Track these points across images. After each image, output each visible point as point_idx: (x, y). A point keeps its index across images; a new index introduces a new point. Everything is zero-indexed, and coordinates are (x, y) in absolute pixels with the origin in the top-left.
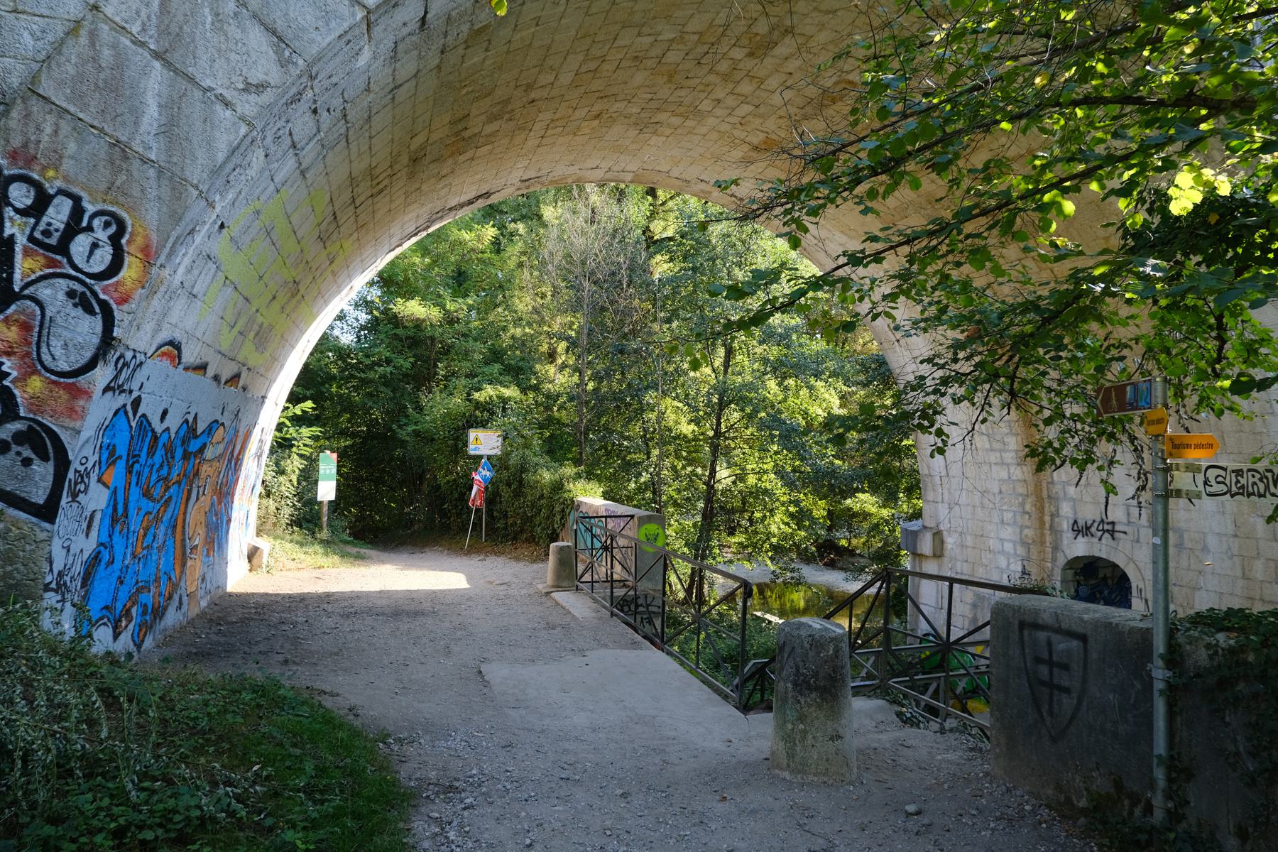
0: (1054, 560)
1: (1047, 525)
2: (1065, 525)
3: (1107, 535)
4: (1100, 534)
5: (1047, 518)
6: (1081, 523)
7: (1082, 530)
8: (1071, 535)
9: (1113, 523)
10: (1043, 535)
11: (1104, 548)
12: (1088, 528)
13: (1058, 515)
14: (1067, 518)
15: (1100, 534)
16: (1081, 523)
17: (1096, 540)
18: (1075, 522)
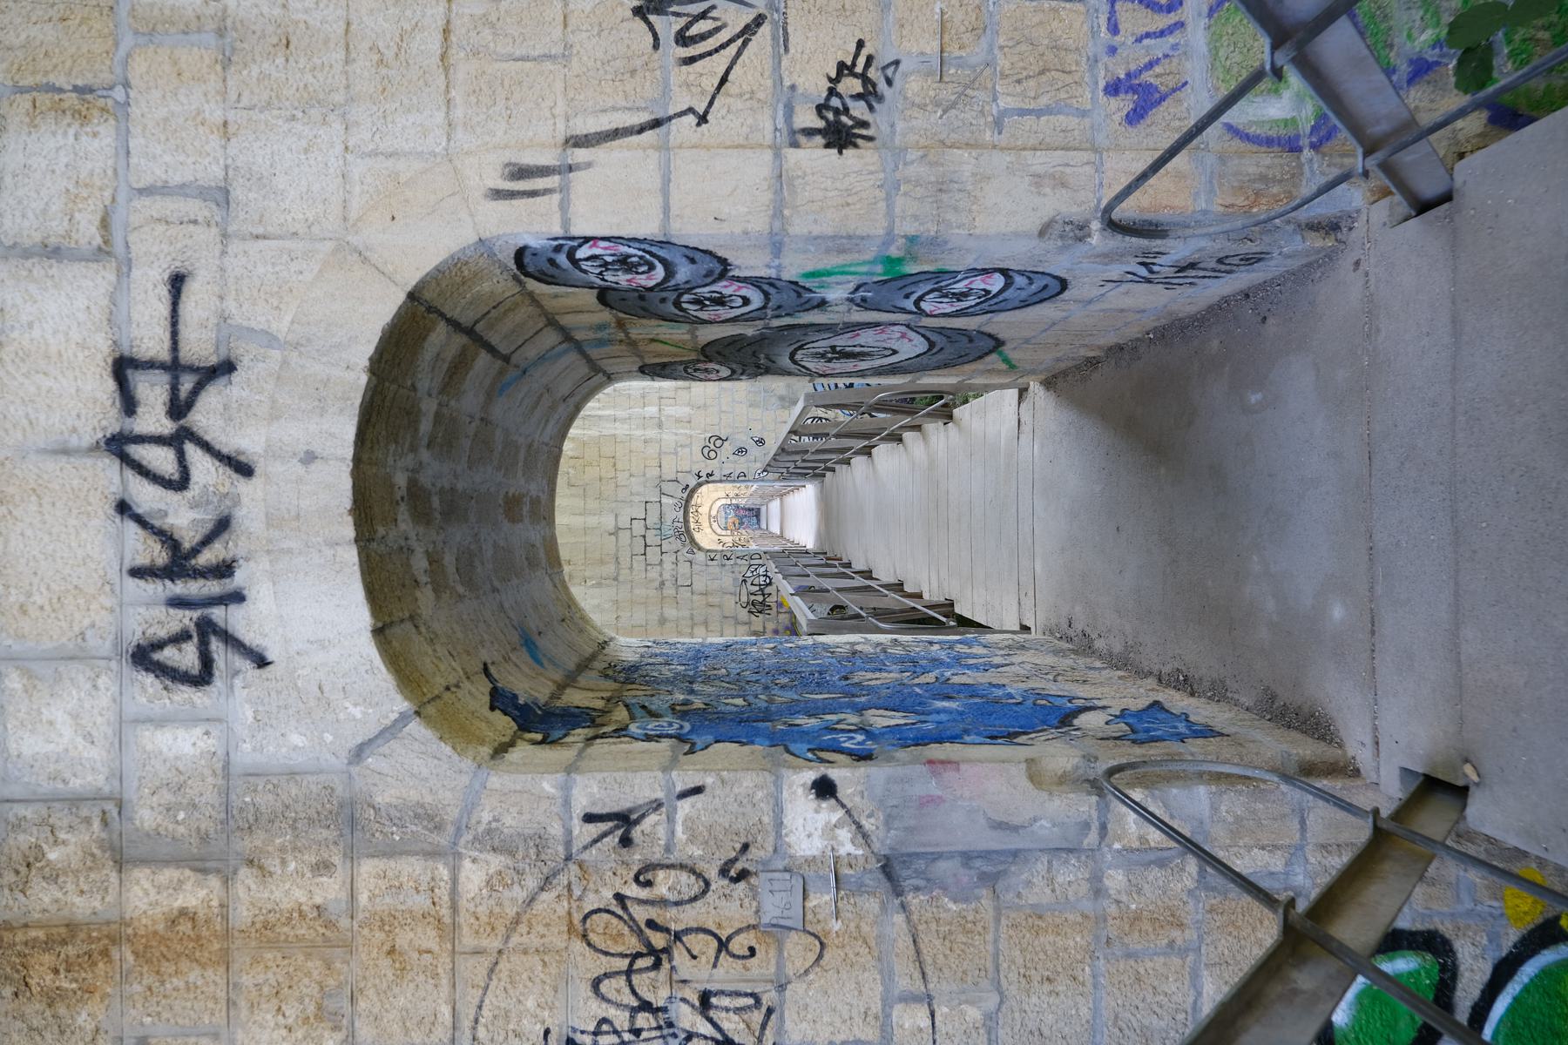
0: (432, 834)
1: (196, 894)
2: (179, 740)
3: (207, 416)
4: (203, 468)
5: (147, 896)
6: (149, 611)
7: (194, 627)
8: (238, 694)
9: (123, 367)
10: (268, 932)
11: (296, 432)
12: (179, 562)
13: (111, 807)
14: (124, 725)
15: (203, 468)
16: (149, 611)
17: (251, 499)
18: (144, 657)
